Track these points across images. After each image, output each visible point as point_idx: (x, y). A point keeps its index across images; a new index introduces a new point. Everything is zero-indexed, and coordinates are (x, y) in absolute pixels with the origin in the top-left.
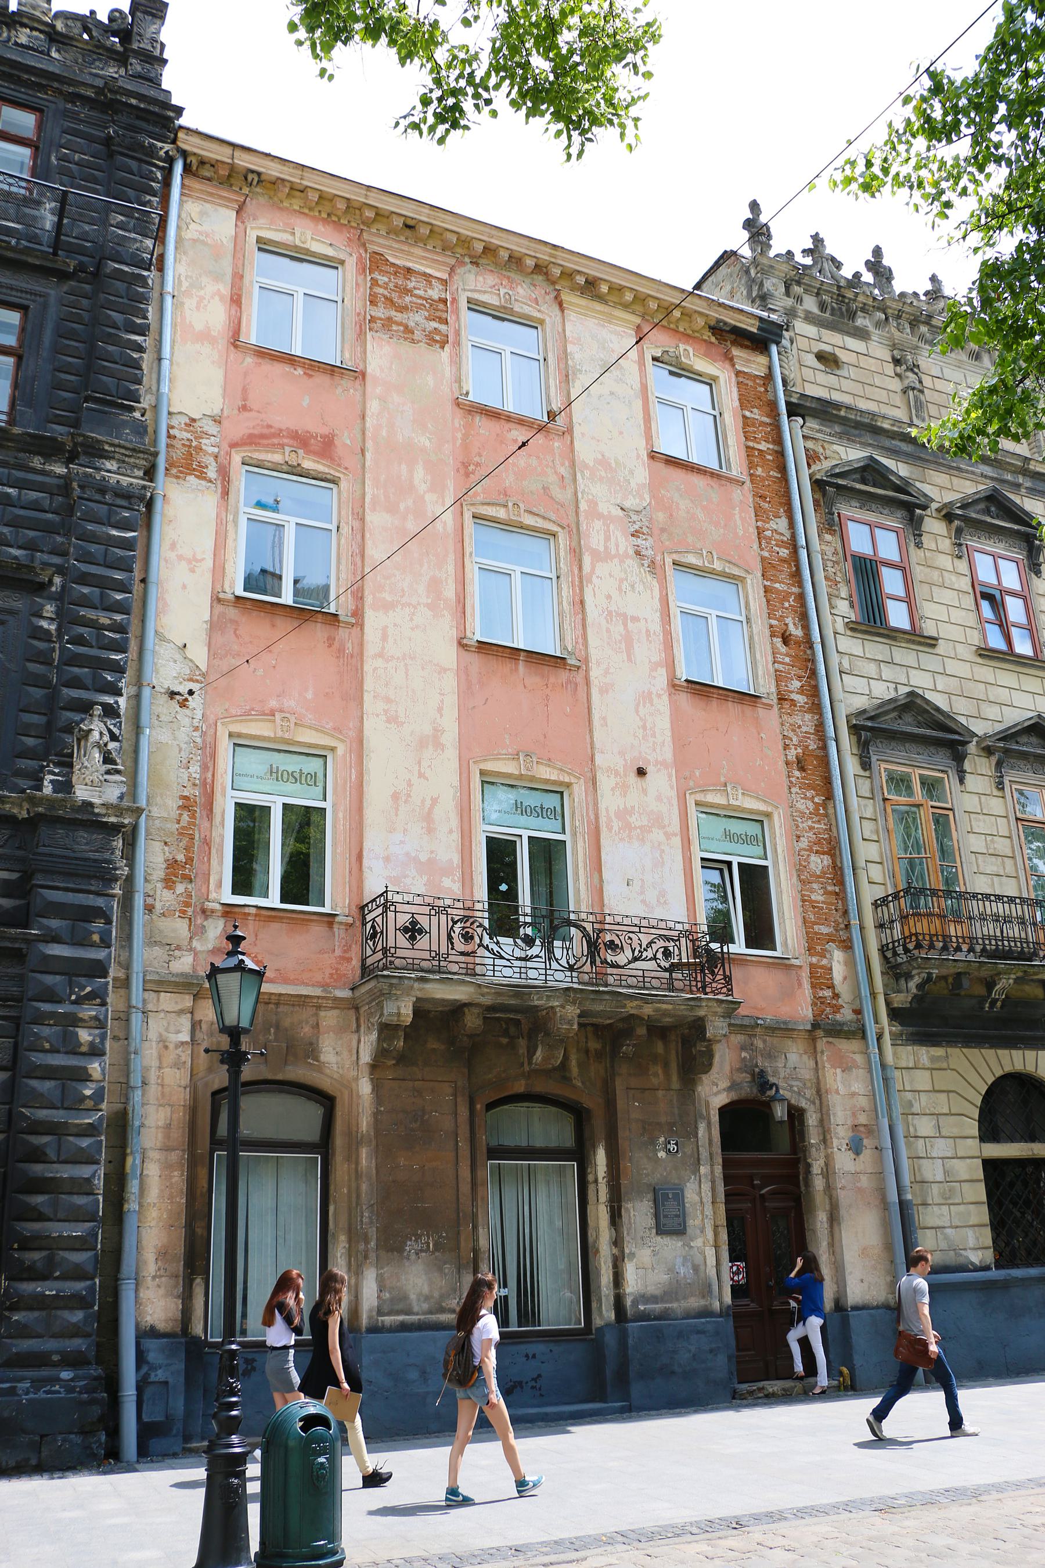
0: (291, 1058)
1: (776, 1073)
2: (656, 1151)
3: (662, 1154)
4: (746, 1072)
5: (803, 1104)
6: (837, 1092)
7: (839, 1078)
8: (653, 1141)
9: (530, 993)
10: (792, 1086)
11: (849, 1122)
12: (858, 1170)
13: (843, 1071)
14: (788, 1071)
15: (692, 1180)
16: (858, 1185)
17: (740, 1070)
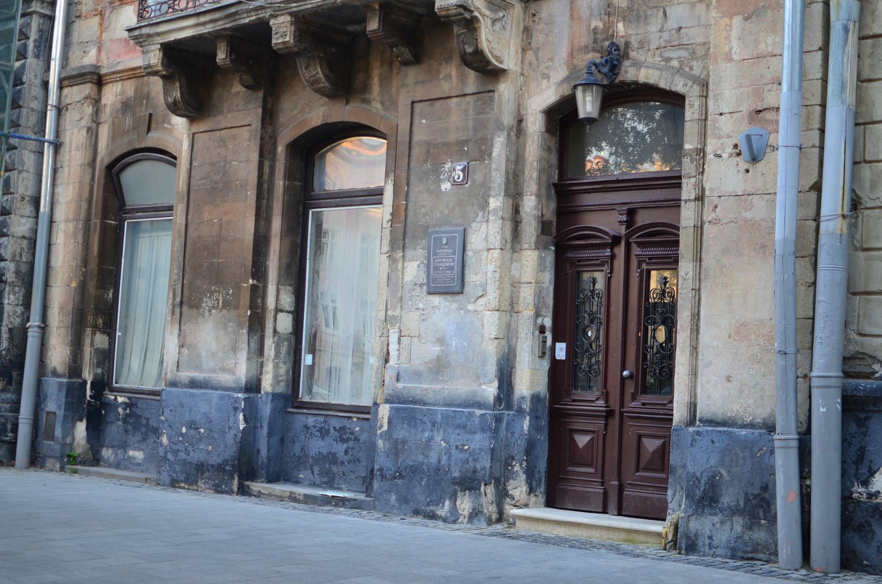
0: (153, 125)
1: (642, 45)
2: (439, 181)
3: (446, 186)
4: (594, 50)
5: (679, 86)
6: (729, 58)
7: (735, 33)
8: (436, 170)
9: (236, 13)
10: (669, 59)
11: (746, 107)
12: (750, 190)
13: (746, 19)
14: (666, 36)
15: (478, 219)
16: (748, 215)
17: (585, 49)
